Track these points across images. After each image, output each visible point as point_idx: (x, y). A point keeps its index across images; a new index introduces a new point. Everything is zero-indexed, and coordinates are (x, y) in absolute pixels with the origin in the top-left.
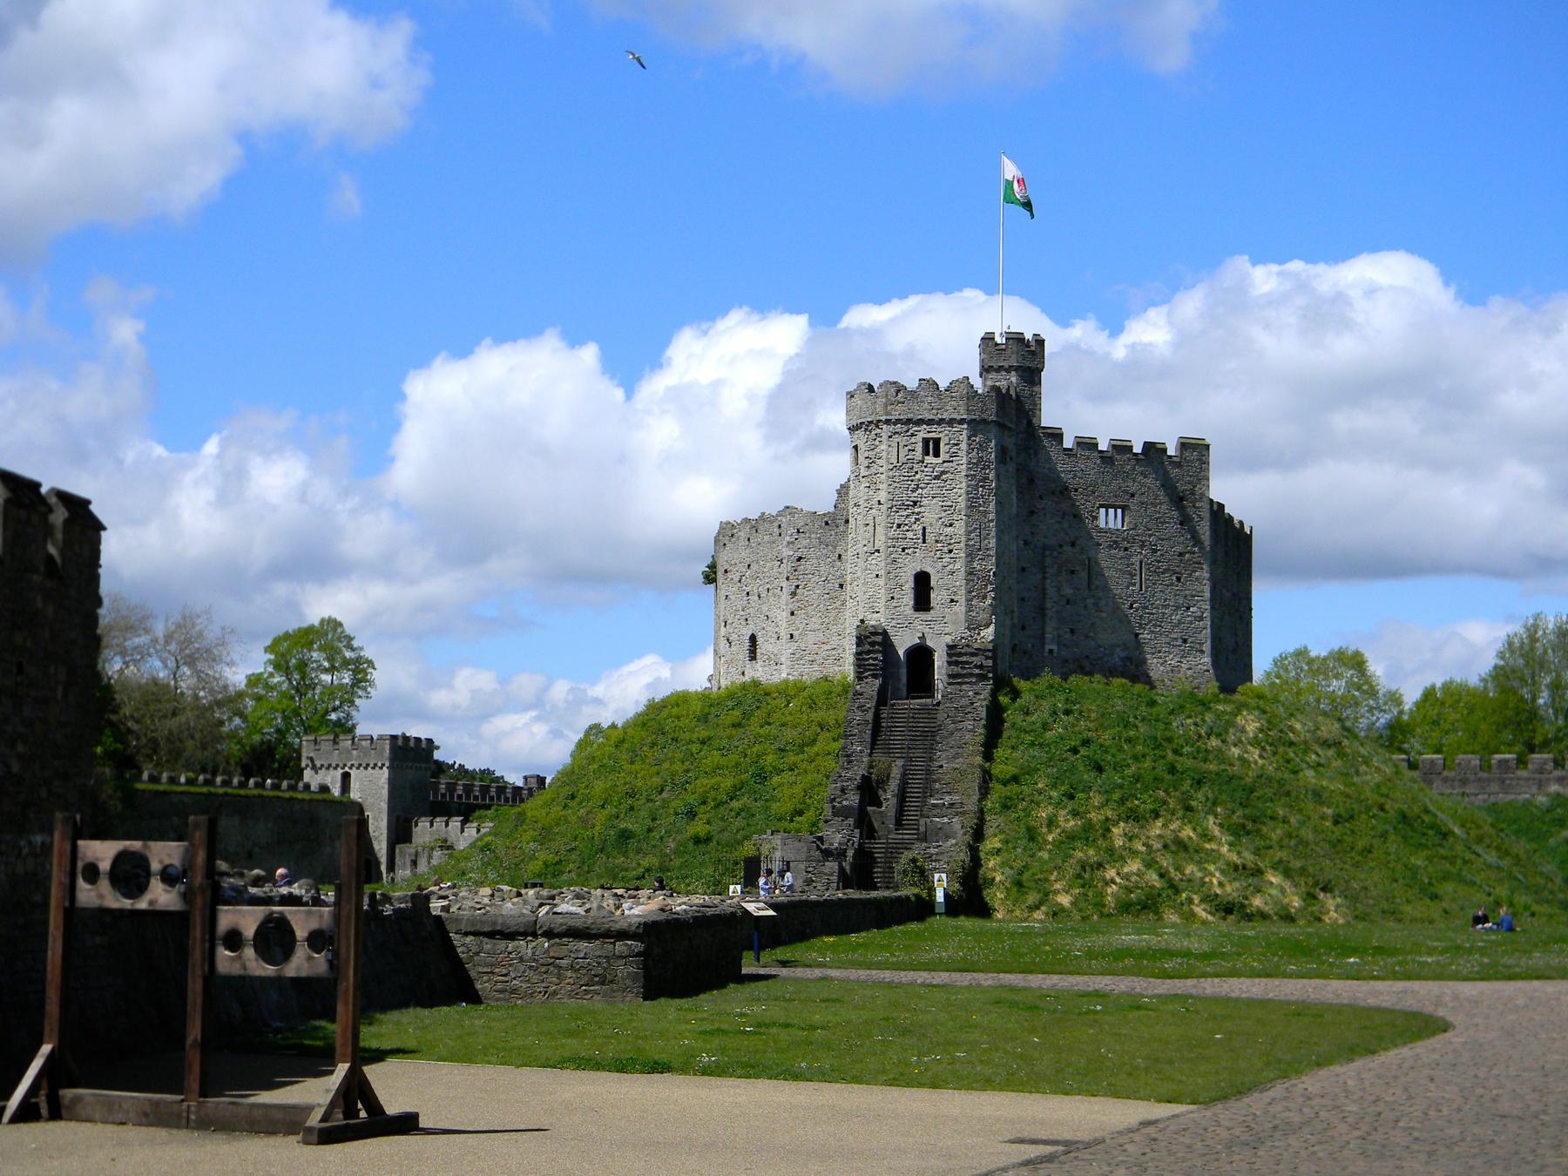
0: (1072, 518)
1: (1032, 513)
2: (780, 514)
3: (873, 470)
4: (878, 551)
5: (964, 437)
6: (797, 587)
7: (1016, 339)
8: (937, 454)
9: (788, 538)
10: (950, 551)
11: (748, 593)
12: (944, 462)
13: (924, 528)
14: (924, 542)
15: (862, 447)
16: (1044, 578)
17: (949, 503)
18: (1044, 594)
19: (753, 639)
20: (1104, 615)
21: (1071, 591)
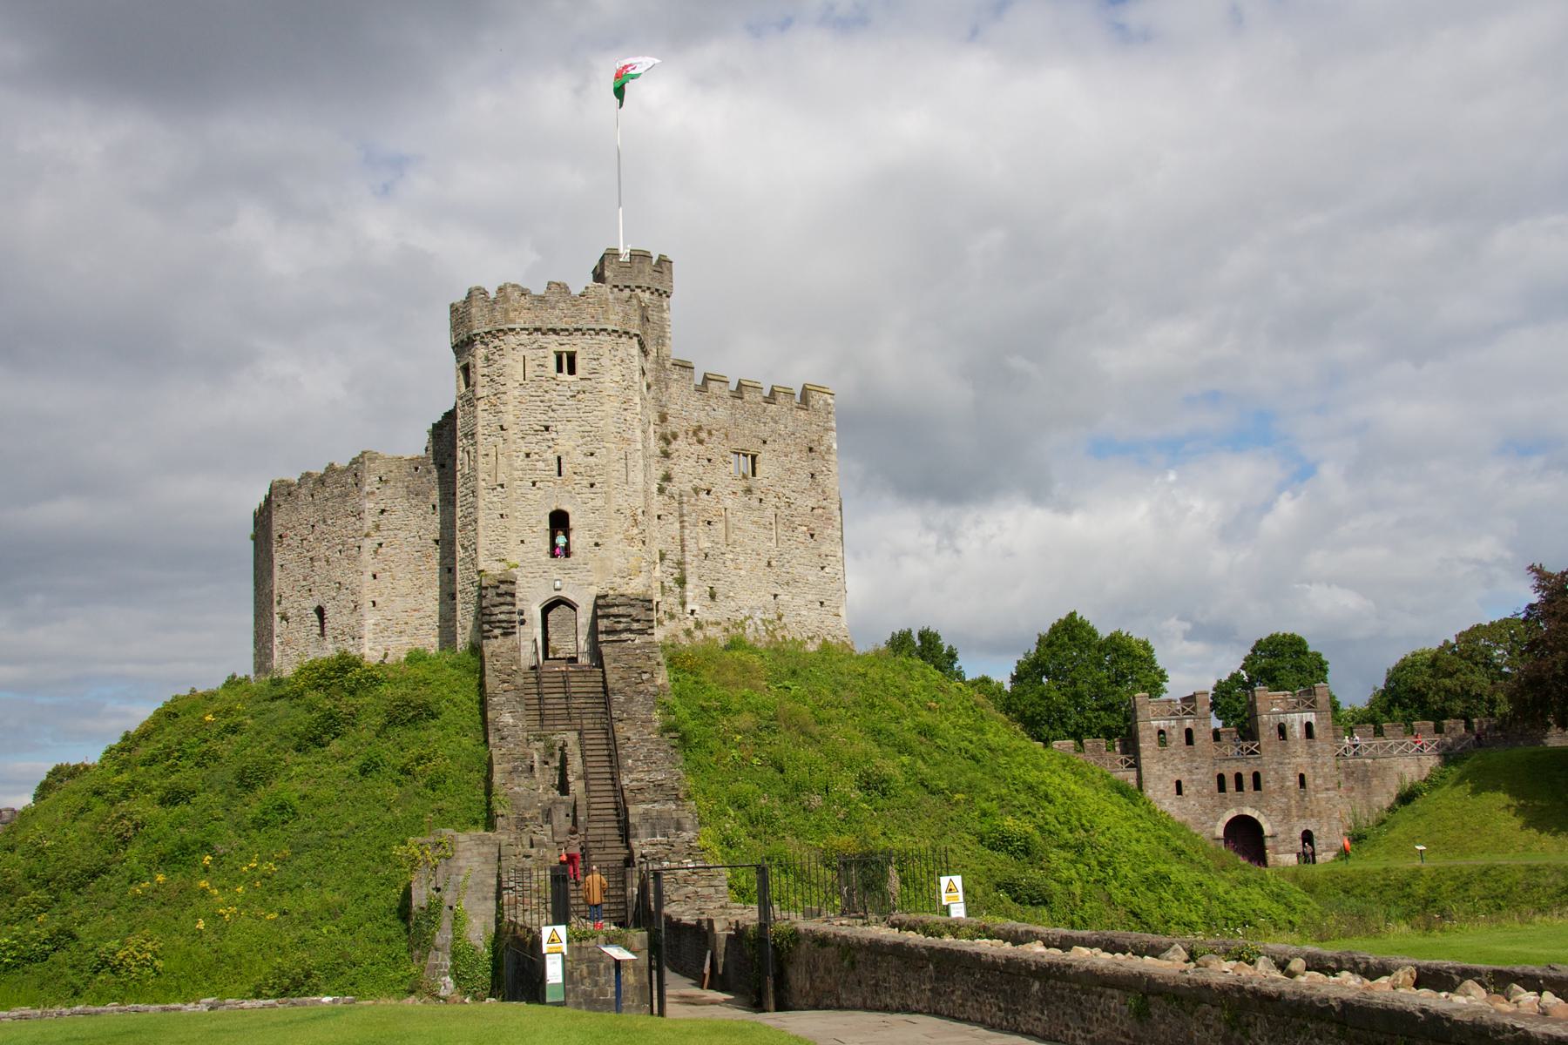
0: (706, 462)
2: (355, 461)
5: (605, 350)
6: (380, 545)
7: (640, 256)
8: (572, 371)
9: (367, 488)
10: (592, 485)
11: (311, 559)
13: (559, 459)
14: (560, 474)
17: (588, 428)
18: (683, 546)
19: (320, 612)
20: (743, 573)
21: (710, 545)
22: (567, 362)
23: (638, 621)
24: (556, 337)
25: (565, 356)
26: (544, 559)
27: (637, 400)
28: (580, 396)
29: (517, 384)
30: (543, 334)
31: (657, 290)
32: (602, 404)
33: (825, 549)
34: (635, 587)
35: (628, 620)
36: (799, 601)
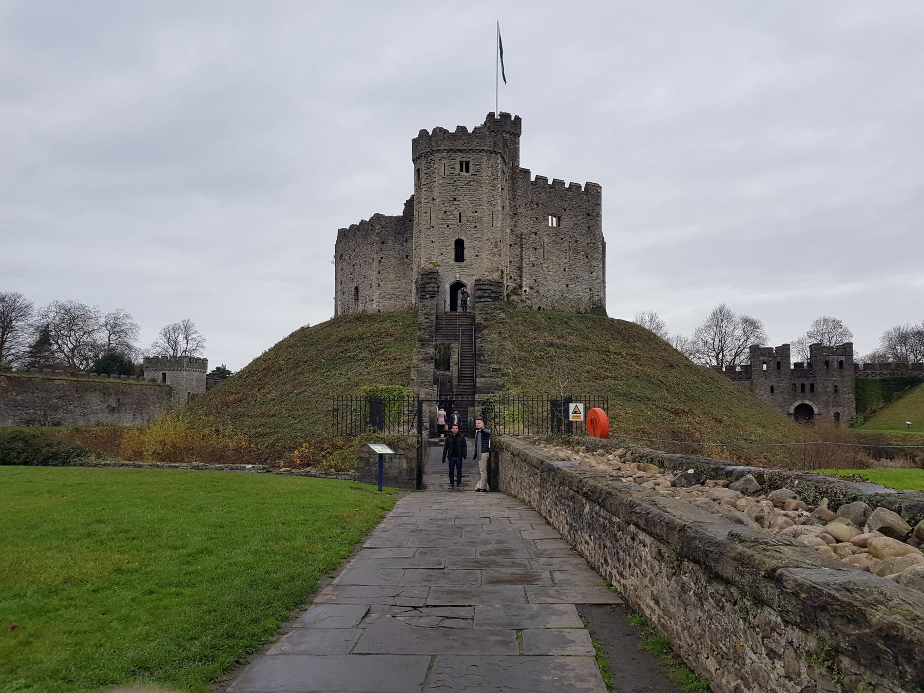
0: (535, 219)
1: (515, 214)
3: (429, 181)
4: (433, 227)
5: (485, 158)
6: (382, 258)
7: (505, 116)
8: (467, 171)
9: (377, 231)
10: (476, 227)
12: (472, 175)
13: (460, 214)
14: (460, 222)
15: (423, 168)
16: (522, 251)
18: (522, 259)
20: (551, 273)
22: (465, 166)
23: (495, 292)
24: (460, 154)
25: (464, 163)
26: (451, 262)
27: (499, 185)
28: (471, 183)
29: (441, 178)
30: (454, 152)
31: (513, 133)
32: (482, 187)
33: (593, 263)
34: (495, 276)
35: (490, 292)
36: (579, 288)
